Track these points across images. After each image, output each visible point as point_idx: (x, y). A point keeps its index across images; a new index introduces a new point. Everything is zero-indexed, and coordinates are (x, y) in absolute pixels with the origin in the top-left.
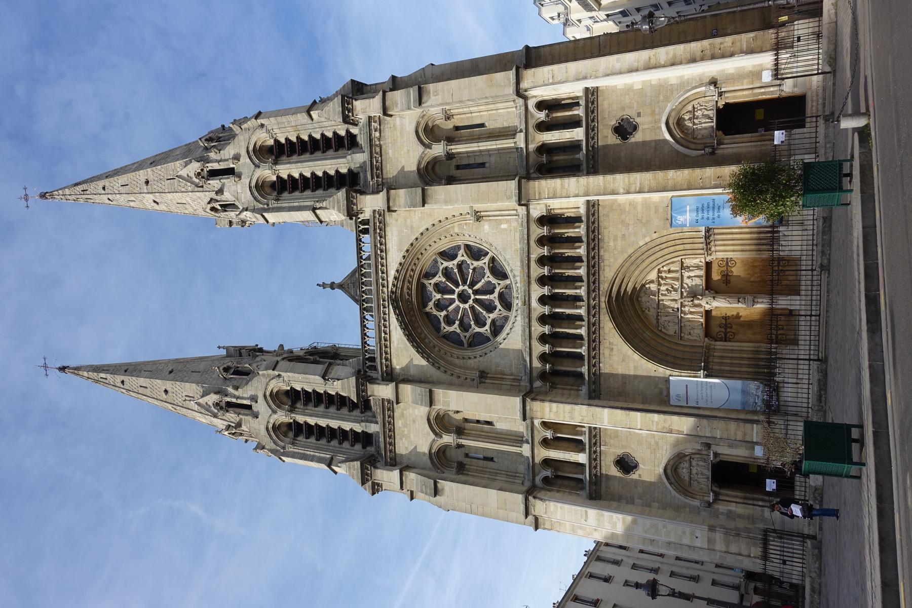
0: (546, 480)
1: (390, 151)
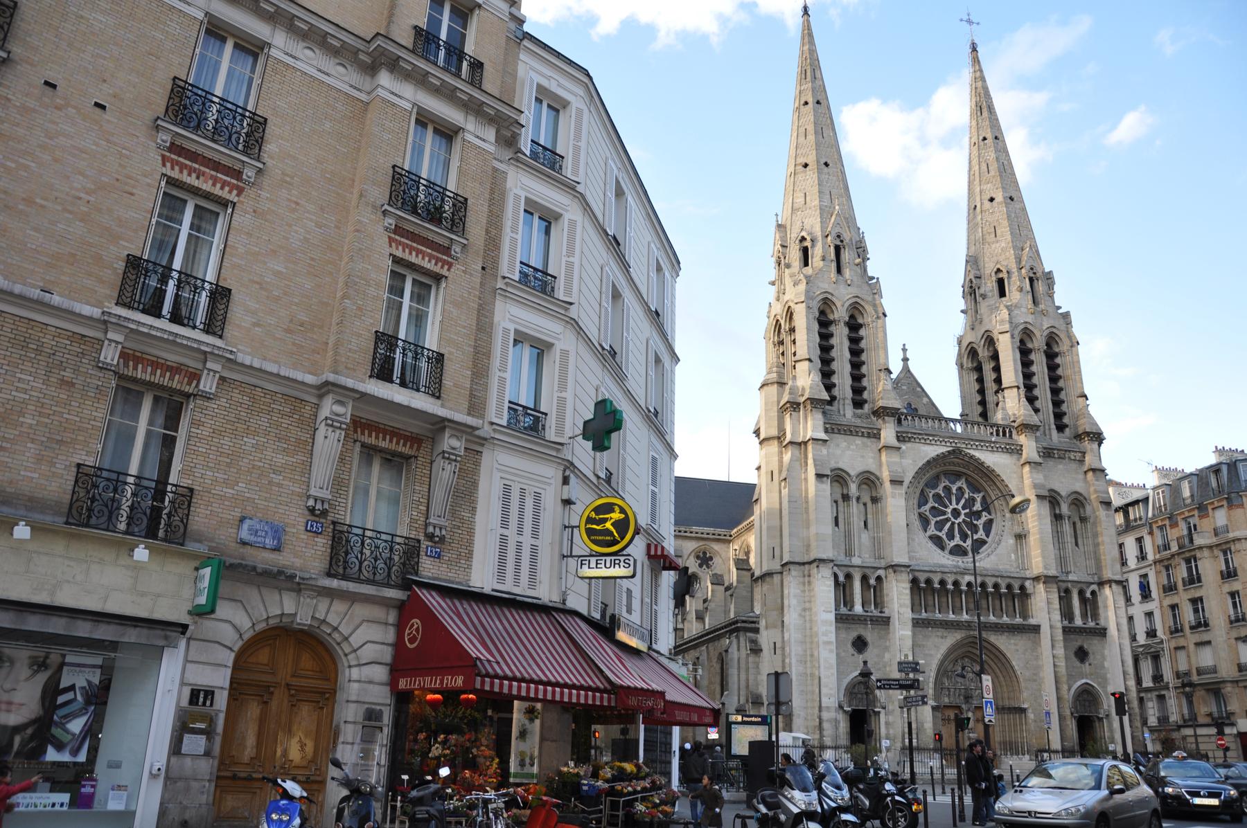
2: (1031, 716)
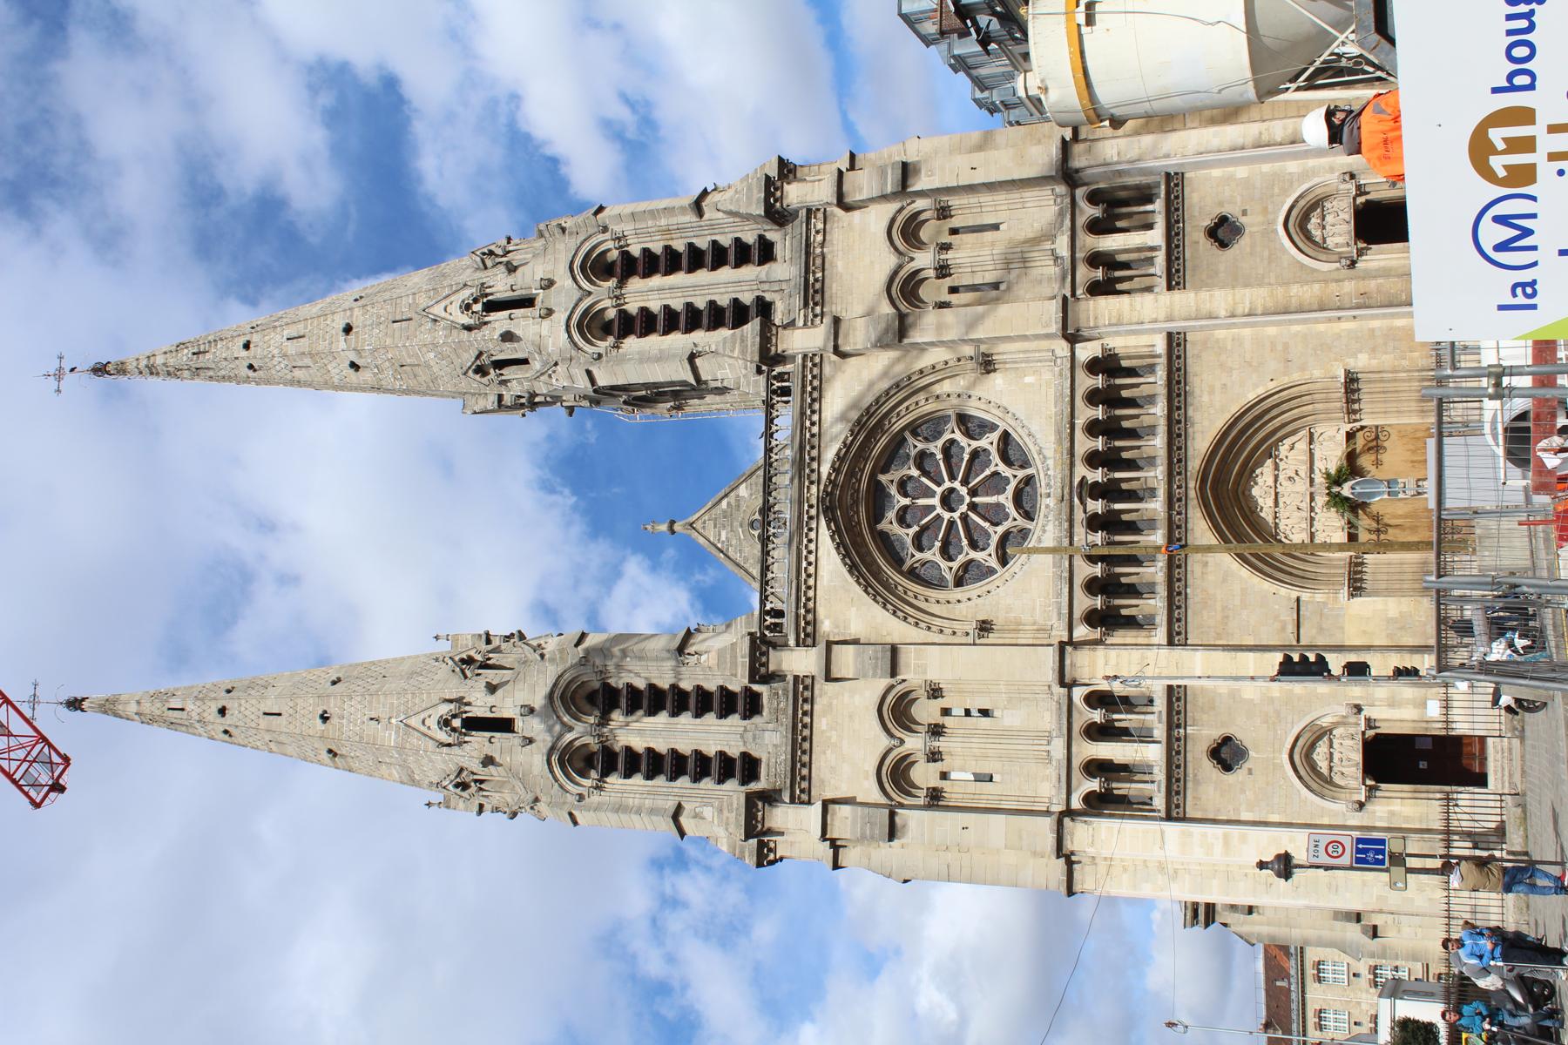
0: (1089, 798)
1: (840, 264)
2: (1361, 362)
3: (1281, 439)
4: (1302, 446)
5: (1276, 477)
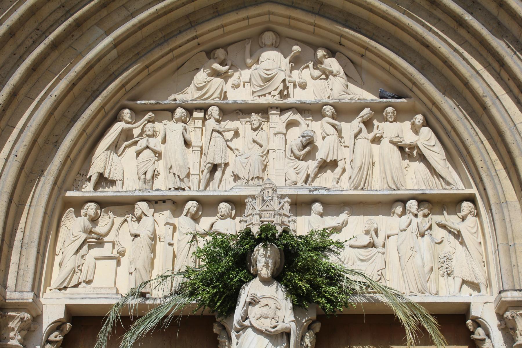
3: (435, 121)
4: (415, 179)
5: (311, 111)
